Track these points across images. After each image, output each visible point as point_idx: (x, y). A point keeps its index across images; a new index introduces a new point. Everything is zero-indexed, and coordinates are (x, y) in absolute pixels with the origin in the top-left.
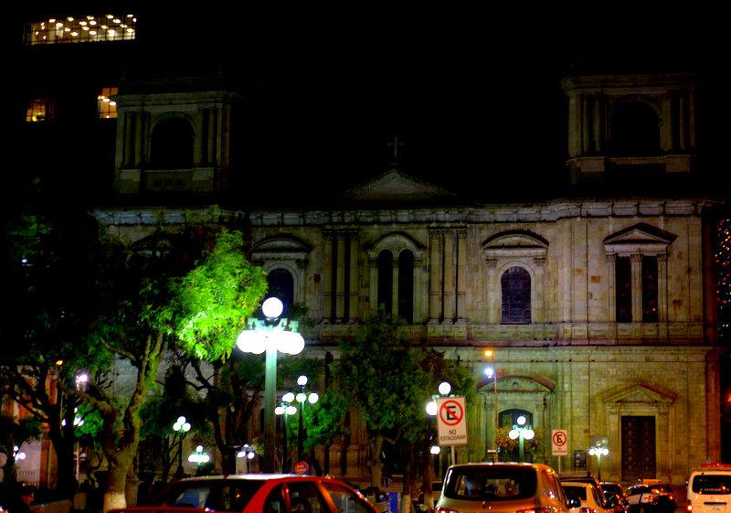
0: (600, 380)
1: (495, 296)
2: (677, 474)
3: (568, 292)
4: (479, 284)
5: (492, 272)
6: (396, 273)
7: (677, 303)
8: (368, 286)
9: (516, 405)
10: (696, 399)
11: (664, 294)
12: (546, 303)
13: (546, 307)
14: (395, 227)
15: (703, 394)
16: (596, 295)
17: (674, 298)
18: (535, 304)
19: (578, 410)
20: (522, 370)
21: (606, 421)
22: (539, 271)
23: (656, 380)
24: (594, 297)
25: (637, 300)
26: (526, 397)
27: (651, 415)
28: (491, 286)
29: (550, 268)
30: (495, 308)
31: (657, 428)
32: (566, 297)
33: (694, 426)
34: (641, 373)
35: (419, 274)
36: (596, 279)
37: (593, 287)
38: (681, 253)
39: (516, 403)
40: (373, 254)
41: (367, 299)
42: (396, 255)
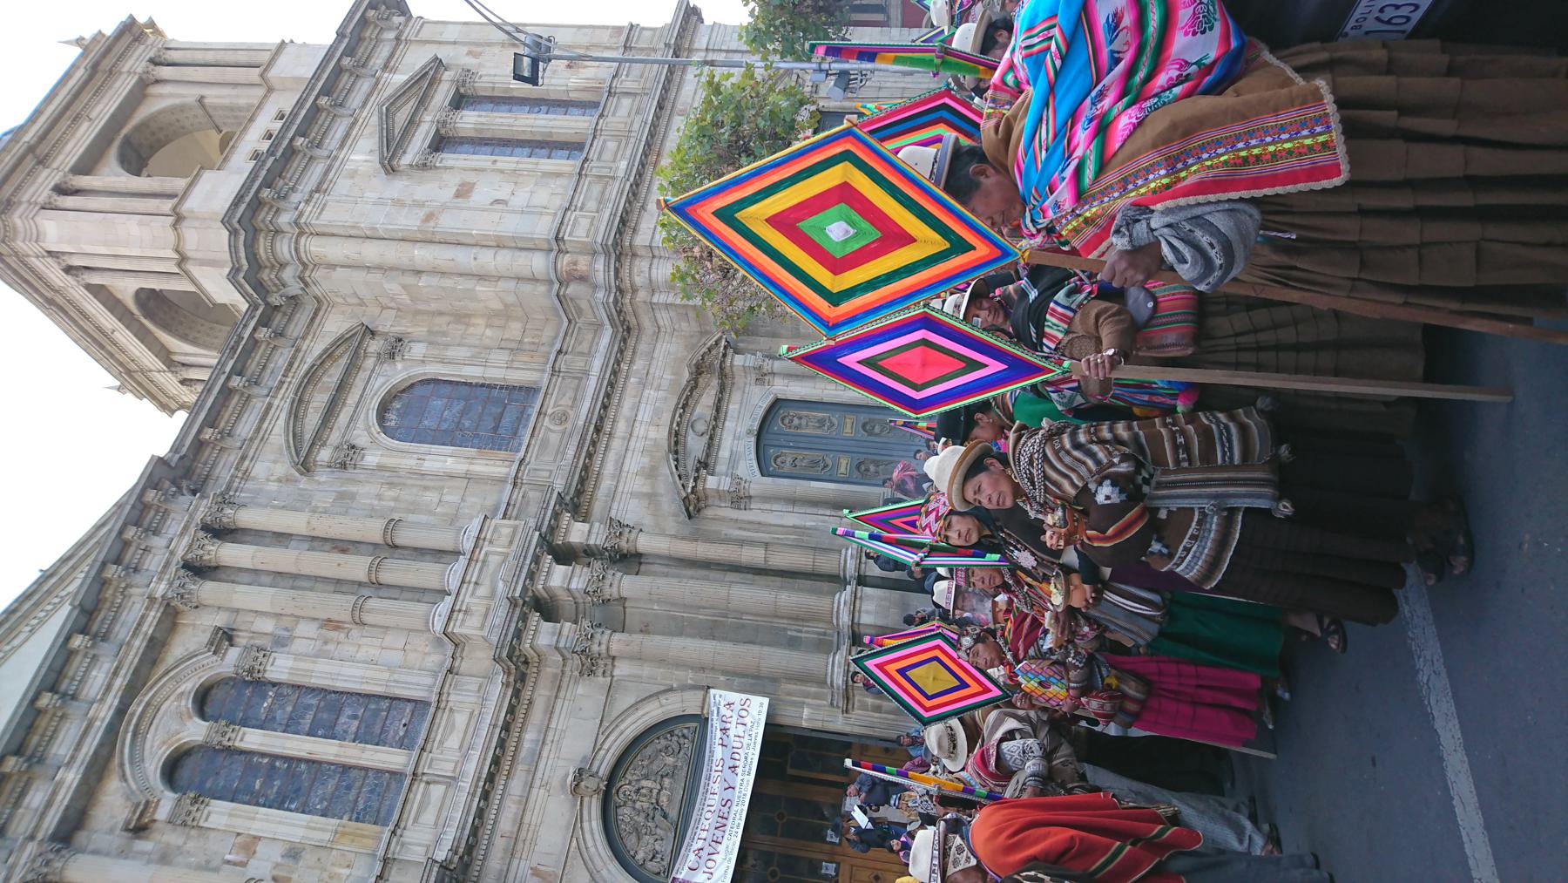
1: (443, 459)
3: (475, 250)
5: (371, 459)
6: (253, 739)
8: (250, 845)
9: (749, 432)
12: (503, 344)
13: (513, 345)
14: (105, 713)
16: (503, 194)
18: (496, 370)
20: (657, 412)
22: (418, 350)
26: (733, 407)
28: (409, 462)
29: (418, 330)
32: (489, 260)
35: (280, 668)
36: (464, 191)
37: (484, 192)
38: (470, 53)
39: (742, 429)
40: (167, 802)
41: (294, 853)
42: (197, 731)
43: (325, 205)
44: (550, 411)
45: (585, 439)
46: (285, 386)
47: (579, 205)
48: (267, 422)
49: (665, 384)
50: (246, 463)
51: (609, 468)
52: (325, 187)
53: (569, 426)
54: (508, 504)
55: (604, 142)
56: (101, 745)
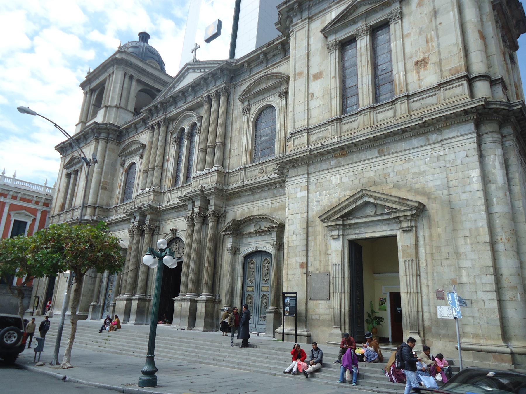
0: (320, 195)
2: (440, 336)
4: (237, 132)
7: (421, 63)
10: (464, 197)
11: (400, 57)
15: (477, 184)
17: (415, 60)
19: (295, 237)
21: (327, 250)
23: (396, 179)
24: (315, 97)
25: (365, 80)
27: (389, 233)
30: (246, 150)
31: (400, 254)
33: (465, 246)
34: (372, 174)
43: (304, 28)
44: (263, 166)
45: (244, 187)
46: (269, 69)
47: (313, 132)
48: (256, 76)
49: (274, 205)
50: (244, 82)
51: (243, 199)
52: (314, 18)
53: (259, 176)
54: (233, 172)
55: (356, 120)
56: (181, 111)
